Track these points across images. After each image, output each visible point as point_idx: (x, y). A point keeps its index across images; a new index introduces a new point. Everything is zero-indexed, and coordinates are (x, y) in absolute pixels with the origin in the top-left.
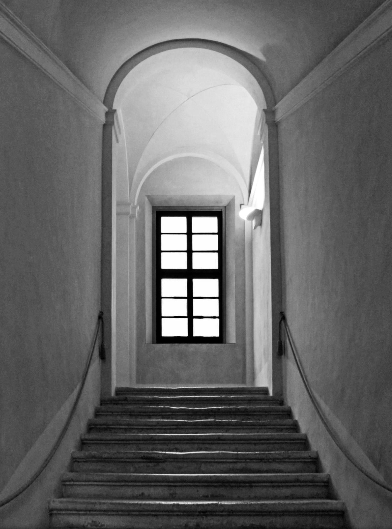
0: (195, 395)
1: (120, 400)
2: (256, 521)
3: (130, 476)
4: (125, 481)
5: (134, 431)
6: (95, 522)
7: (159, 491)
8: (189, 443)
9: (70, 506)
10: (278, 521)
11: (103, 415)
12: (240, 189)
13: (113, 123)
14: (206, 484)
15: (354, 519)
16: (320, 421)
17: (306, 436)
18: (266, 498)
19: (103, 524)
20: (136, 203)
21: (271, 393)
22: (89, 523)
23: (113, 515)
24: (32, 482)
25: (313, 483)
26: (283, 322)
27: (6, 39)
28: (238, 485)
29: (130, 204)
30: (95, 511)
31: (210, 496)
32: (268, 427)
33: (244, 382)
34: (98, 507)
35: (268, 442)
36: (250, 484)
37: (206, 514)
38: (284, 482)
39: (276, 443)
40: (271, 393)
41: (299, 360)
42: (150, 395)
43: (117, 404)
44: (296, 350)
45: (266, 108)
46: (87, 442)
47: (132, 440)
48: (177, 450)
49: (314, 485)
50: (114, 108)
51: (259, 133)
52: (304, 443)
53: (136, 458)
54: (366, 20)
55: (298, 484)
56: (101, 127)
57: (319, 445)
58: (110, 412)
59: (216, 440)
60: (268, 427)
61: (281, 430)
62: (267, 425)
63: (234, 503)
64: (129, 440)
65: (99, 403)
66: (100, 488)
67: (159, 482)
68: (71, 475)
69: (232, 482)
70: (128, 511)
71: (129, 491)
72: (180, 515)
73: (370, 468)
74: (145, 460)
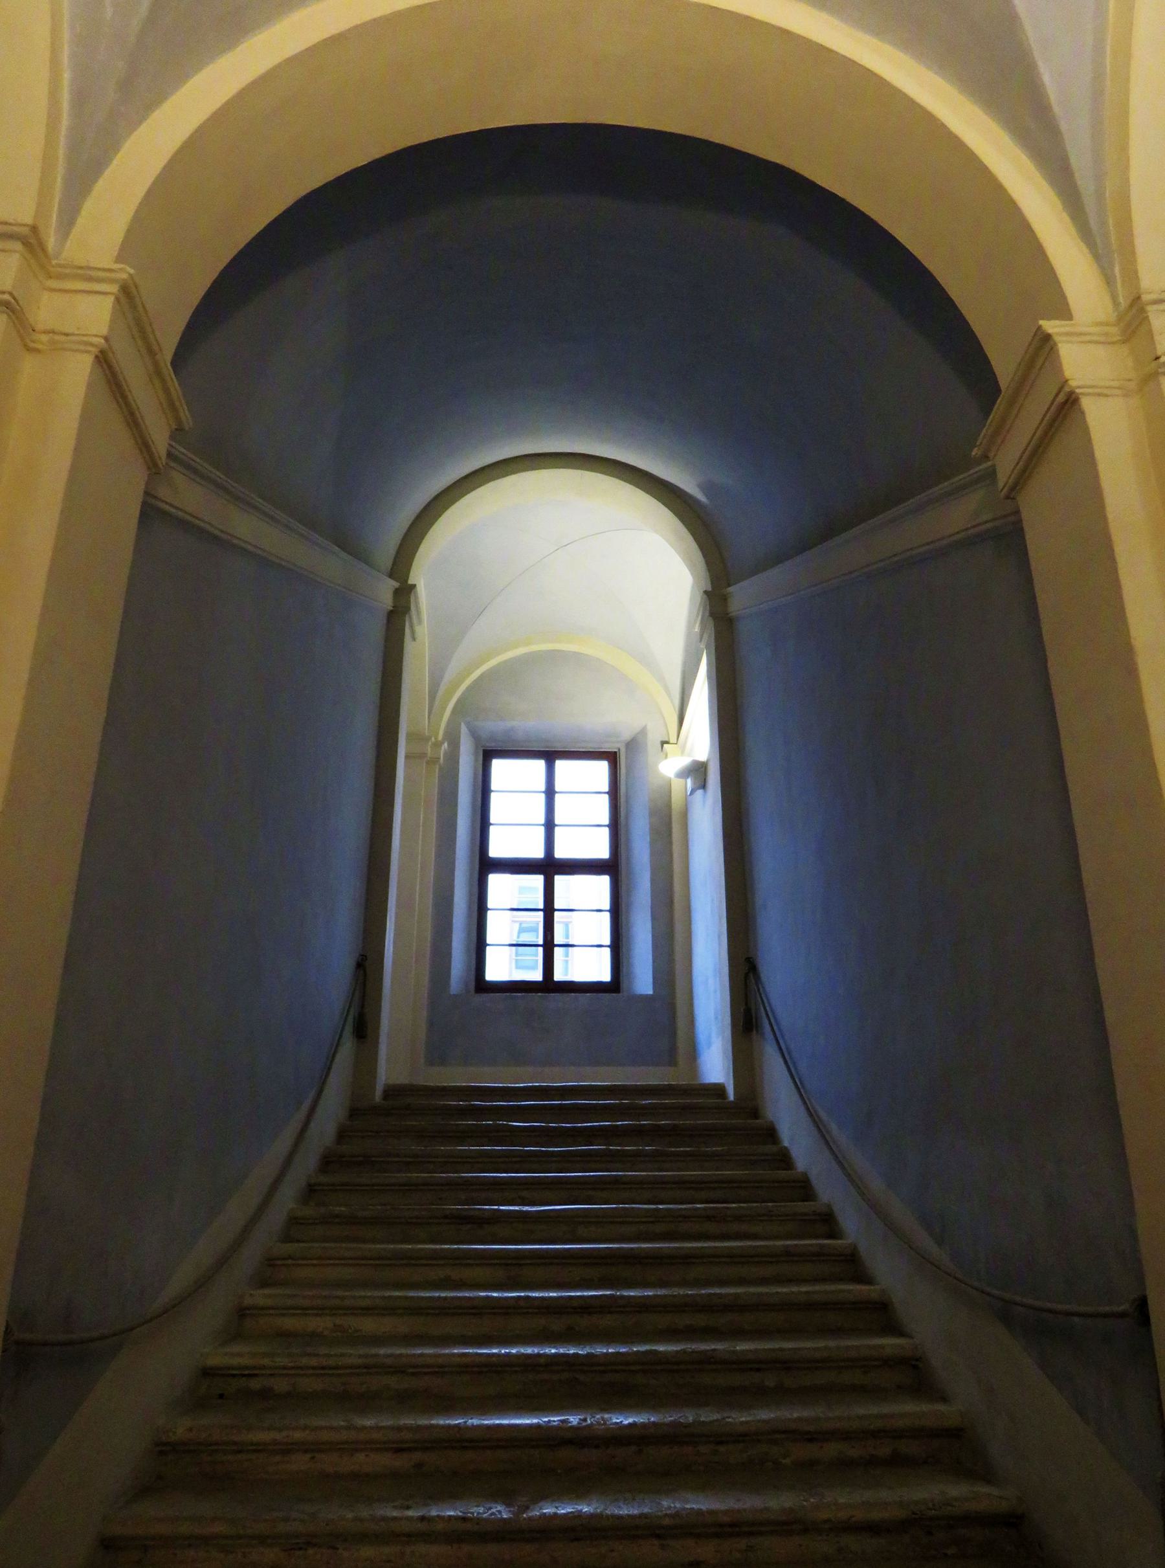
17: (805, 1174)
52: (803, 1188)
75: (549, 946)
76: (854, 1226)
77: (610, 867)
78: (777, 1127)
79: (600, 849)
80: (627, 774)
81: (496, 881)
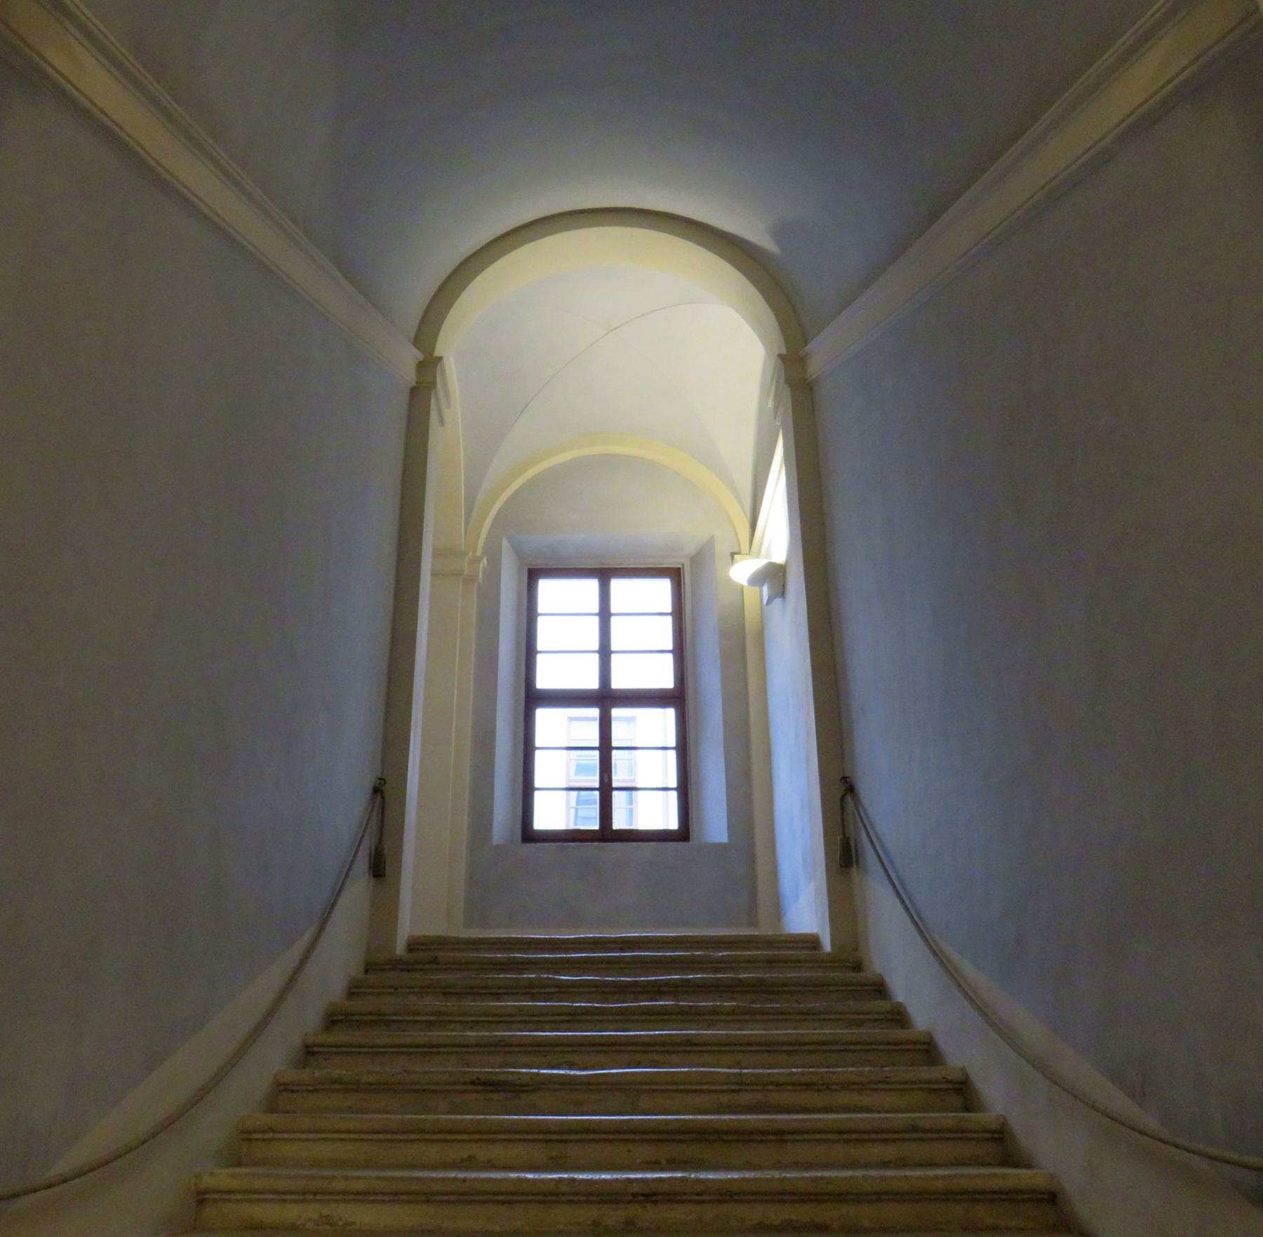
0: (622, 950)
1: (417, 963)
2: (804, 1213)
3: (438, 1120)
4: (423, 1131)
5: (452, 1026)
6: (327, 1217)
7: (519, 1151)
8: (605, 1052)
9: (258, 1185)
10: (865, 1214)
11: (371, 994)
12: (731, 522)
13: (433, 385)
14: (654, 1137)
15: (1085, 1209)
16: (966, 1003)
18: (826, 1166)
19: (350, 1220)
20: (479, 552)
21: (827, 945)
22: (310, 1220)
23: (383, 1202)
24: (154, 1135)
25: (960, 1134)
26: (849, 798)
27: (206, 211)
28: (746, 1137)
29: (464, 554)
30: (331, 1193)
31: (664, 1162)
32: (822, 1016)
33: (753, 922)
34: (339, 1185)
35: (824, 1048)
36: (781, 1136)
37: (654, 1198)
38: (876, 1132)
39: (846, 1050)
40: (827, 945)
41: (898, 877)
42: (499, 950)
43: (409, 971)
44: (888, 857)
45: (784, 352)
46: (321, 1049)
47: (446, 1046)
48: (571, 1066)
49: (961, 1139)
50: (437, 353)
51: (770, 405)
52: (928, 1051)
53: (455, 1083)
54: (994, 167)
55: (915, 1135)
56: (406, 394)
57: (966, 1050)
58: (391, 987)
59: (680, 1044)
60: (822, 1016)
61: (860, 1024)
62: (821, 1013)
63: (735, 1175)
64: (439, 1046)
65: (362, 969)
66: (350, 1146)
67: (519, 1132)
68: (269, 1119)
69: (727, 1133)
70: (425, 1194)
71: (433, 1152)
72: (579, 1202)
73: (1121, 1103)
74: (480, 1088)
75: (606, 789)
76: (999, 1095)
77: (675, 698)
78: (887, 979)
79: (662, 676)
80: (693, 593)
81: (545, 717)
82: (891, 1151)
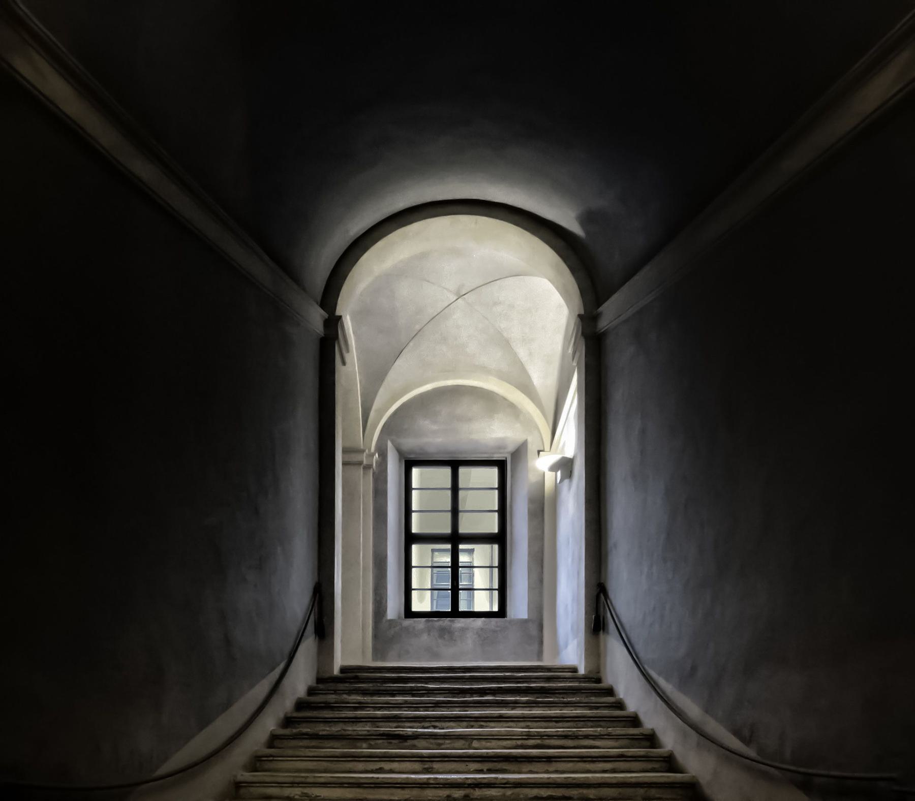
10: (591, 793)
34: (309, 780)
36: (549, 759)
40: (582, 671)
48: (435, 727)
52: (634, 721)
57: (654, 719)
61: (597, 708)
66: (315, 763)
82: (608, 766)
